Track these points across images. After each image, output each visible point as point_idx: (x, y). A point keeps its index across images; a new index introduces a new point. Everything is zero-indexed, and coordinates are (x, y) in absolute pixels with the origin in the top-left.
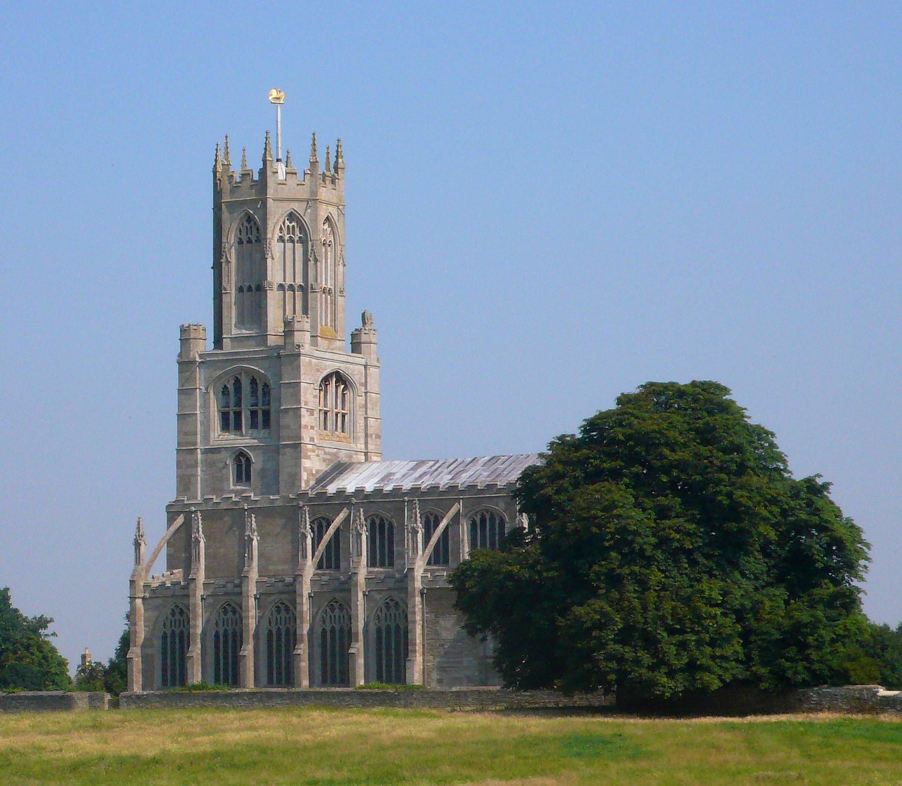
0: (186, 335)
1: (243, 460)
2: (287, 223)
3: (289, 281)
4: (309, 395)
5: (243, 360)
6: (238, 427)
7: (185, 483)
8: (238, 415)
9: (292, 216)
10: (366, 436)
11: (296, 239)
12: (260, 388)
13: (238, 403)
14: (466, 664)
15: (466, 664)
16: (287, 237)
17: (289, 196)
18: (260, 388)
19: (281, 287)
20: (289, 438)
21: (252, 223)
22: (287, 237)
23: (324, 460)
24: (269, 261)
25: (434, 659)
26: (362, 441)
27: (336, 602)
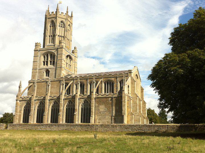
0: (37, 45)
1: (48, 72)
2: (61, 23)
3: (61, 35)
4: (64, 57)
5: (49, 50)
6: (47, 65)
7: (33, 76)
8: (47, 62)
9: (62, 22)
10: (74, 71)
11: (63, 27)
12: (53, 56)
13: (47, 59)
14: (107, 118)
15: (107, 118)
16: (61, 26)
17: (62, 17)
18: (53, 56)
19: (59, 36)
20: (59, 66)
21: (53, 23)
22: (61, 26)
23: (66, 73)
24: (57, 29)
25: (98, 116)
26: (74, 72)
27: (71, 101)
